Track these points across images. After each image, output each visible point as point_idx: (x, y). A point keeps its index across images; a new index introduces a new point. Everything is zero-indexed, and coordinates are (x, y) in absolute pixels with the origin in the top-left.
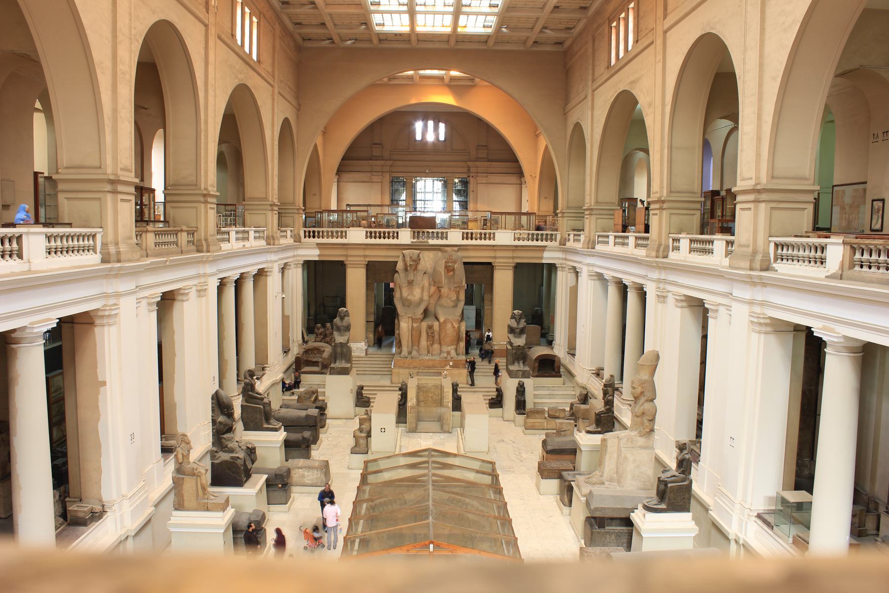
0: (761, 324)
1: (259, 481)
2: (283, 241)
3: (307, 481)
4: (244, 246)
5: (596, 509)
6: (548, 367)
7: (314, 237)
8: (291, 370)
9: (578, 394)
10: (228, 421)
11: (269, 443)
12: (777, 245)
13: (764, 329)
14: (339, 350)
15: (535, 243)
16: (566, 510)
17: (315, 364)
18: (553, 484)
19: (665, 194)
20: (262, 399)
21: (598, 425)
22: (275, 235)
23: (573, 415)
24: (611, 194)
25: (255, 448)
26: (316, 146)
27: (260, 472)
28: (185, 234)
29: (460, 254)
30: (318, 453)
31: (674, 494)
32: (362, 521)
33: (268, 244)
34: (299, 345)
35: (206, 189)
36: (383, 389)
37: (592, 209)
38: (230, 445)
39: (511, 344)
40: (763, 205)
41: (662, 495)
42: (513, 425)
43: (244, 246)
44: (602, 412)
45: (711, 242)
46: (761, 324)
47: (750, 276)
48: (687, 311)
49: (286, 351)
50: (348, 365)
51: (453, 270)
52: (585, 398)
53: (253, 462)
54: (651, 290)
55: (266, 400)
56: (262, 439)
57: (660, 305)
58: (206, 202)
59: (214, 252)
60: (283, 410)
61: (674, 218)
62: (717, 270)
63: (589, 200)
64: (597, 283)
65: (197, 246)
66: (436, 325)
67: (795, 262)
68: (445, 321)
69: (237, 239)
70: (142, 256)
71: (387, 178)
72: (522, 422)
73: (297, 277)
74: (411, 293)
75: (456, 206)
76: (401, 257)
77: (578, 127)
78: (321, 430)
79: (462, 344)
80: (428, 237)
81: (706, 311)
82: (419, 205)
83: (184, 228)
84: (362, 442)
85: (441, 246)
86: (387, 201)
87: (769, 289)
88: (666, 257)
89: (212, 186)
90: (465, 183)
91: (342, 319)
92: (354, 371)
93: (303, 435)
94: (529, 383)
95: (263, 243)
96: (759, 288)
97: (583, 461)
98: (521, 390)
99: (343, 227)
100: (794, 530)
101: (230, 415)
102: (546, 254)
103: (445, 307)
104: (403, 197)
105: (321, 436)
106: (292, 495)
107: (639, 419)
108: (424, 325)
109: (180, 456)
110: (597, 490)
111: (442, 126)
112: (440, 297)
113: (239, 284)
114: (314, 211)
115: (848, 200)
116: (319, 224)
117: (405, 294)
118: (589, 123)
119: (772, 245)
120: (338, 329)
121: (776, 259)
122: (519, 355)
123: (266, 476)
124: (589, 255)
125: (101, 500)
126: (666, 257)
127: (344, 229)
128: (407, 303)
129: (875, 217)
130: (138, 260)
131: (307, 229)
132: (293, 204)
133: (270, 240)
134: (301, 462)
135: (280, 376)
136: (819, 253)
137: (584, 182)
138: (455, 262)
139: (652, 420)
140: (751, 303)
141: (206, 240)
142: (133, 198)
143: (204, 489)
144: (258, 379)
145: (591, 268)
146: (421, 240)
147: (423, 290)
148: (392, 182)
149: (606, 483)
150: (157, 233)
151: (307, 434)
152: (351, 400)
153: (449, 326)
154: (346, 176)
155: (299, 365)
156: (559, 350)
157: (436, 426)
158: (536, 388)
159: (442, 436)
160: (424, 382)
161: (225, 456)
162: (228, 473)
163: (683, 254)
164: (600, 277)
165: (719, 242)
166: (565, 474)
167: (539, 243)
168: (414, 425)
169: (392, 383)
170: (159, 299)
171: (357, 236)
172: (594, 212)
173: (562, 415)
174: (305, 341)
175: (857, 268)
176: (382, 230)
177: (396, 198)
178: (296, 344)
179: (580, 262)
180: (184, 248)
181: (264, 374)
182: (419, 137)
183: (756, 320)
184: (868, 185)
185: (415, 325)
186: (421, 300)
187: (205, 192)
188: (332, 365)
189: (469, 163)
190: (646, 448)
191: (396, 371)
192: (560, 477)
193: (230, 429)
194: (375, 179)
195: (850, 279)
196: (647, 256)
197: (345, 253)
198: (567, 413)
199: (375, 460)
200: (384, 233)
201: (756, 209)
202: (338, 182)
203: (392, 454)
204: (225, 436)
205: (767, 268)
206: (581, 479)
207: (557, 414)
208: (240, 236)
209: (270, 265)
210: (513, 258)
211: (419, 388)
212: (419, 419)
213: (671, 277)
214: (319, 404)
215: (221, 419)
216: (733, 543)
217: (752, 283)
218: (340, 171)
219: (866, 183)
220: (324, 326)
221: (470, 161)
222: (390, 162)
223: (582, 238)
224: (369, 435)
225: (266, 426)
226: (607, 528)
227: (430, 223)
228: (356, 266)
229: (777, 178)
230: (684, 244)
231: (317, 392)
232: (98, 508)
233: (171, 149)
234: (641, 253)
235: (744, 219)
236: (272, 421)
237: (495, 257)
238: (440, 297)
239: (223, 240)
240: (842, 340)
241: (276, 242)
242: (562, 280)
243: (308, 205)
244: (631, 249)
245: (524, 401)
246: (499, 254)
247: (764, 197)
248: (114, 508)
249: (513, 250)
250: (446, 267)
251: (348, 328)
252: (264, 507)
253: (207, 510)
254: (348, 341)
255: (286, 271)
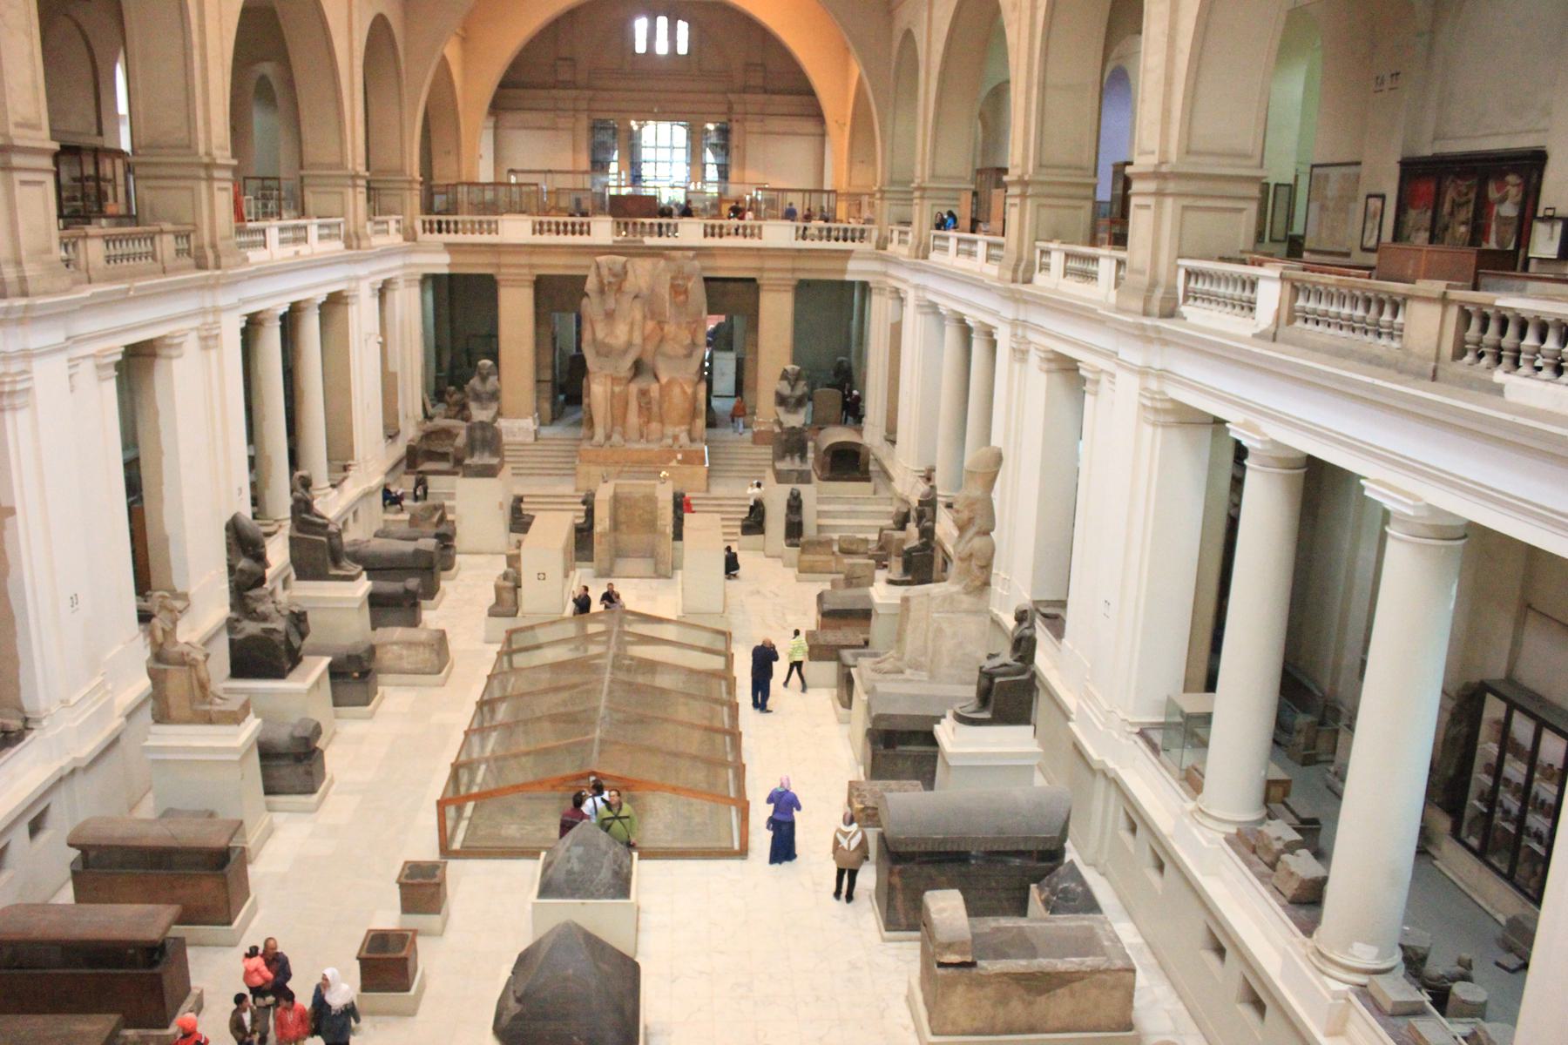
0: (1156, 410)
1: (316, 668)
2: (379, 241)
3: (406, 665)
4: (297, 253)
5: (878, 719)
6: (848, 463)
7: (440, 231)
8: (403, 467)
9: (892, 509)
10: (256, 567)
11: (340, 603)
12: (1189, 274)
13: (1162, 419)
14: (478, 434)
15: (833, 245)
16: (845, 711)
17: (443, 457)
18: (829, 669)
19: (1031, 170)
20: (325, 526)
21: (907, 570)
22: (360, 231)
23: (881, 548)
24: (958, 163)
25: (304, 613)
26: (444, 64)
27: (318, 652)
28: (171, 238)
29: (697, 263)
30: (432, 616)
31: (1008, 695)
32: (494, 734)
33: (348, 247)
34: (418, 424)
35: (208, 154)
36: (556, 503)
37: (921, 189)
38: (261, 608)
39: (780, 424)
40: (1169, 202)
41: (984, 697)
42: (779, 563)
43: (297, 253)
44: (914, 549)
45: (1095, 259)
46: (1156, 410)
47: (1143, 327)
48: (1056, 377)
49: (391, 435)
50: (495, 461)
51: (686, 292)
52: (902, 522)
53: (303, 636)
54: (1003, 336)
55: (332, 528)
56: (327, 594)
57: (1017, 366)
58: (210, 179)
59: (229, 267)
60: (378, 541)
61: (1045, 212)
62: (1093, 311)
63: (921, 173)
64: (931, 319)
65: (196, 258)
66: (654, 389)
67: (1214, 306)
68: (670, 383)
69: (282, 241)
70: (76, 283)
71: (584, 122)
72: (795, 560)
73: (410, 307)
74: (611, 333)
75: (712, 173)
76: (593, 269)
77: (908, 34)
78: (443, 574)
79: (701, 422)
80: (642, 234)
81: (1084, 380)
82: (647, 171)
83: (167, 226)
84: (508, 596)
85: (667, 248)
86: (584, 162)
87: (1168, 350)
88: (1028, 281)
89: (221, 148)
90: (724, 132)
91: (484, 379)
92: (507, 471)
93: (405, 583)
94: (808, 492)
95: (337, 246)
96: (1156, 348)
97: (879, 630)
98: (795, 505)
99: (496, 213)
100: (1189, 757)
101: (260, 558)
102: (852, 265)
103: (670, 357)
104: (615, 157)
105: (443, 584)
106: (380, 689)
107: (965, 565)
108: (633, 388)
109: (159, 634)
110: (886, 686)
111: (683, 27)
112: (662, 340)
113: (290, 321)
114: (445, 182)
115: (1332, 190)
116: (452, 208)
117: (600, 335)
118: (925, 27)
119: (1182, 273)
120: (478, 397)
121: (1186, 298)
122: (792, 444)
123: (327, 660)
124: (918, 271)
125: (21, 709)
126: (1028, 281)
127: (493, 218)
128: (605, 351)
129: (1369, 225)
130: (67, 291)
131: (427, 218)
132: (401, 171)
133: (352, 240)
134: (398, 633)
135: (377, 480)
136: (1247, 293)
137: (914, 138)
138: (689, 278)
139: (987, 567)
140: (1144, 372)
141: (214, 246)
142: (50, 180)
143: (203, 687)
144: (333, 486)
145: (921, 293)
146: (630, 237)
147: (632, 324)
148: (596, 127)
149: (908, 672)
150: (108, 240)
151: (413, 583)
152: (498, 523)
153: (677, 391)
154: (510, 118)
155: (412, 459)
156: (871, 435)
157: (644, 565)
158: (820, 501)
159: (655, 583)
160: (626, 490)
161: (251, 628)
162: (261, 656)
163: (1052, 280)
164: (934, 308)
165: (1107, 257)
166: (847, 655)
167: (841, 245)
168: (606, 565)
169: (577, 490)
170: (119, 357)
171: (516, 229)
172: (928, 194)
173: (862, 549)
174: (428, 417)
175: (1299, 324)
176: (562, 219)
177: (600, 157)
178: (413, 422)
179: (904, 281)
180: (169, 263)
181: (344, 479)
182: (641, 47)
183: (1148, 403)
184: (1364, 170)
185: (617, 389)
186: (630, 344)
187: (206, 160)
188: (467, 461)
189: (732, 97)
190: (976, 612)
191: (583, 469)
192: (838, 658)
193: (261, 580)
194: (562, 122)
195: (1287, 342)
196: (1000, 279)
197: (494, 261)
198: (873, 546)
199: (532, 628)
200: (565, 224)
201: (1159, 206)
202: (496, 128)
203: (557, 617)
204: (251, 593)
205: (1170, 313)
206: (866, 663)
207: (854, 547)
208: (290, 235)
209: (353, 285)
210: (794, 270)
211: (616, 500)
212: (618, 553)
213: (1036, 317)
214: (443, 529)
215: (244, 563)
216: (1099, 776)
217: (1146, 337)
218: (498, 107)
219: (1358, 164)
220: (461, 389)
221: (733, 92)
222: (588, 93)
223: (910, 238)
224: (517, 586)
225: (333, 572)
226: (900, 748)
227: (649, 207)
228: (515, 283)
229: (1198, 153)
230: (1057, 260)
231: (442, 507)
232: (15, 724)
233: (138, 85)
234: (992, 270)
235: (1140, 222)
236: (346, 563)
237: (760, 270)
238: (662, 340)
239: (253, 245)
240: (1268, 447)
241: (364, 243)
242: (879, 311)
243: (436, 172)
244: (978, 264)
245: (800, 524)
246: (769, 264)
247: (1171, 186)
248: (45, 723)
249: (794, 258)
250: (673, 286)
251: (495, 396)
252: (321, 709)
253: (210, 721)
254: (494, 420)
255: (389, 295)
